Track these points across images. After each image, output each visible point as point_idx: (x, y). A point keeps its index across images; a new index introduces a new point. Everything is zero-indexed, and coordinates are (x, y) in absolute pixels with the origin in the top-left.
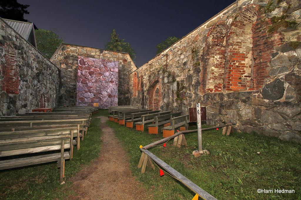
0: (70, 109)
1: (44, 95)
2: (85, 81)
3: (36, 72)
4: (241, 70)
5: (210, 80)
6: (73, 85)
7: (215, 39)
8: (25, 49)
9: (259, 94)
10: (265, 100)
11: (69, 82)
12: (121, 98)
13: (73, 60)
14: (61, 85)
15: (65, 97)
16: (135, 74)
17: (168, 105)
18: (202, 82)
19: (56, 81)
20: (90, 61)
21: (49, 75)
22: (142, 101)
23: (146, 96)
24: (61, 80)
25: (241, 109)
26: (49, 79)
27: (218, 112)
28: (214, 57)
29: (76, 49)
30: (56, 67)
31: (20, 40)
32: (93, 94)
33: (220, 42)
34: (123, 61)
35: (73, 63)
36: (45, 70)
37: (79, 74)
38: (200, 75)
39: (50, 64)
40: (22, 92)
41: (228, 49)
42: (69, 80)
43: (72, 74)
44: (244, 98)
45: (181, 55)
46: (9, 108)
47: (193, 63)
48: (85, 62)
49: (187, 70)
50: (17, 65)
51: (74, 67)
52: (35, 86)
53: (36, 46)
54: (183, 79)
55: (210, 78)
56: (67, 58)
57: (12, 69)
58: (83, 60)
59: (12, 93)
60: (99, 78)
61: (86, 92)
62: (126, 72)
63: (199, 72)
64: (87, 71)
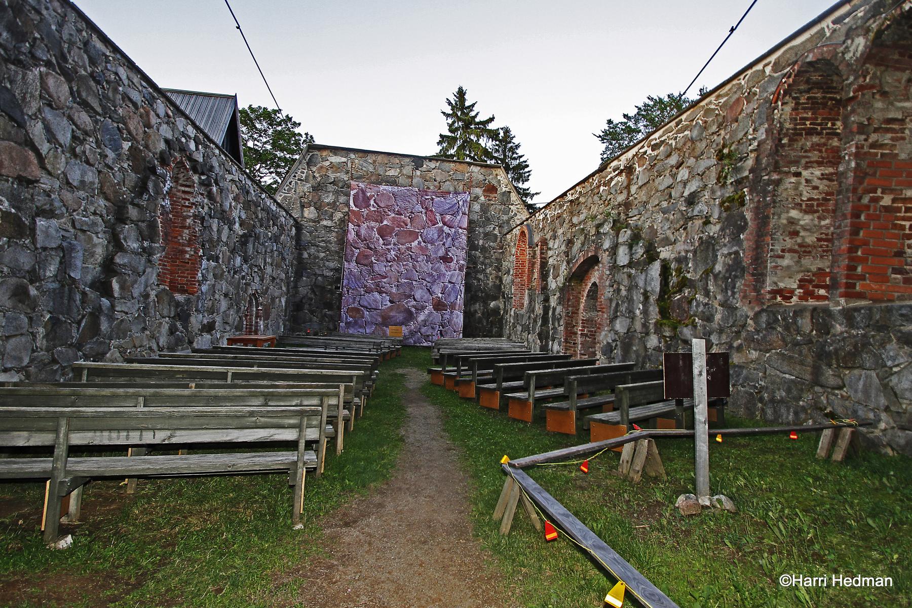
0: (322, 339)
1: (256, 299)
2: (367, 257)
3: (241, 233)
4: (903, 223)
5: (782, 257)
6: (331, 270)
7: (804, 109)
8: (217, 169)
11: (322, 260)
12: (476, 311)
13: (337, 193)
14: (301, 267)
16: (523, 233)
17: (627, 341)
18: (751, 264)
19: (289, 257)
20: (383, 194)
21: (270, 239)
22: (541, 326)
23: (554, 309)
25: (895, 369)
26: (272, 251)
27: (808, 377)
28: (798, 175)
29: (344, 160)
30: (291, 216)
31: (206, 147)
32: (388, 298)
33: (823, 119)
34: (484, 191)
35: (334, 202)
36: (261, 226)
37: (352, 236)
38: (747, 240)
39: (274, 209)
40: (204, 288)
41: (849, 148)
42: (322, 255)
43: (333, 237)
45: (677, 168)
46: (172, 331)
47: (722, 196)
49: (698, 223)
50: (195, 216)
51: (338, 215)
52: (235, 273)
53: (243, 159)
54: (683, 254)
55: (783, 251)
56: (317, 188)
57: (184, 227)
58: (363, 192)
59: (183, 291)
60: (408, 249)
61: (368, 291)
62: (494, 229)
63: (742, 229)
64: (373, 224)
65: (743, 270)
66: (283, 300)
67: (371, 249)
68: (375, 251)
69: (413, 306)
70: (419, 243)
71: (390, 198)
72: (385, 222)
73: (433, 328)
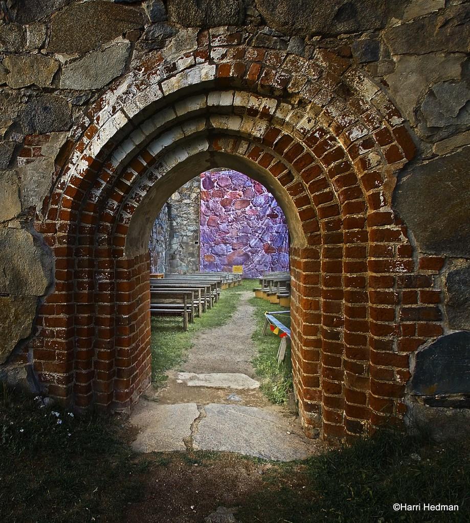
6: (192, 231)
11: (185, 225)
15: (180, 255)
20: (222, 178)
24: (171, 224)
32: (231, 247)
37: (203, 208)
42: (185, 222)
48: (213, 183)
51: (194, 195)
58: (209, 178)
64: (217, 199)
66: (164, 253)
67: (217, 215)
68: (220, 216)
69: (249, 251)
70: (251, 208)
71: (227, 179)
72: (225, 197)
73: (265, 266)
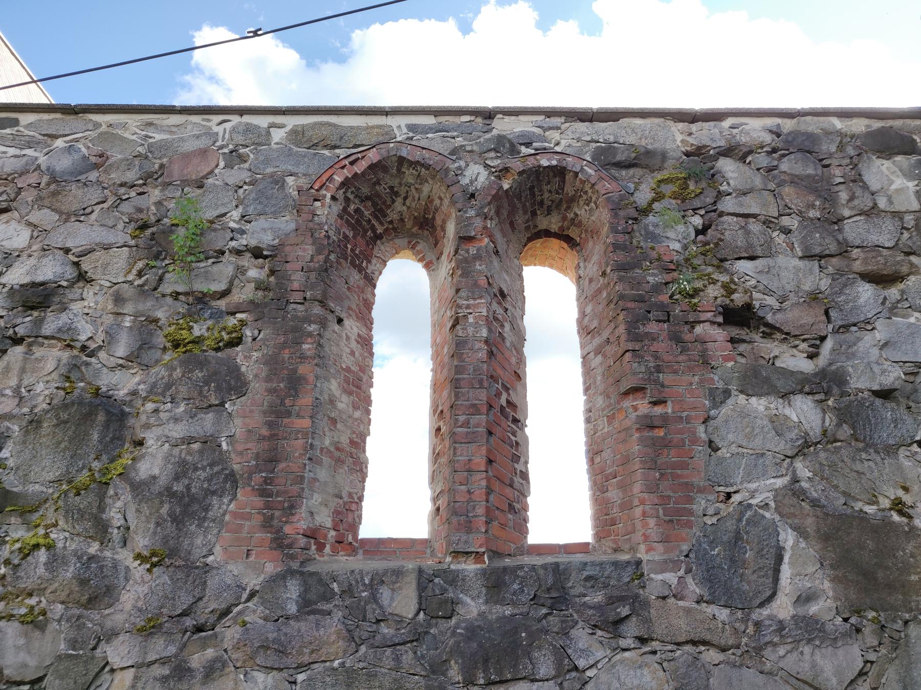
9: (682, 573)
10: (711, 609)
33: (361, 251)
44: (597, 598)
49: (52, 357)
65: (232, 478)
